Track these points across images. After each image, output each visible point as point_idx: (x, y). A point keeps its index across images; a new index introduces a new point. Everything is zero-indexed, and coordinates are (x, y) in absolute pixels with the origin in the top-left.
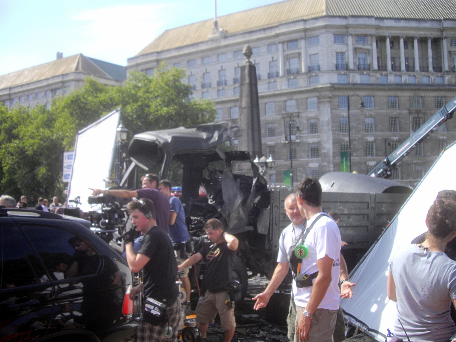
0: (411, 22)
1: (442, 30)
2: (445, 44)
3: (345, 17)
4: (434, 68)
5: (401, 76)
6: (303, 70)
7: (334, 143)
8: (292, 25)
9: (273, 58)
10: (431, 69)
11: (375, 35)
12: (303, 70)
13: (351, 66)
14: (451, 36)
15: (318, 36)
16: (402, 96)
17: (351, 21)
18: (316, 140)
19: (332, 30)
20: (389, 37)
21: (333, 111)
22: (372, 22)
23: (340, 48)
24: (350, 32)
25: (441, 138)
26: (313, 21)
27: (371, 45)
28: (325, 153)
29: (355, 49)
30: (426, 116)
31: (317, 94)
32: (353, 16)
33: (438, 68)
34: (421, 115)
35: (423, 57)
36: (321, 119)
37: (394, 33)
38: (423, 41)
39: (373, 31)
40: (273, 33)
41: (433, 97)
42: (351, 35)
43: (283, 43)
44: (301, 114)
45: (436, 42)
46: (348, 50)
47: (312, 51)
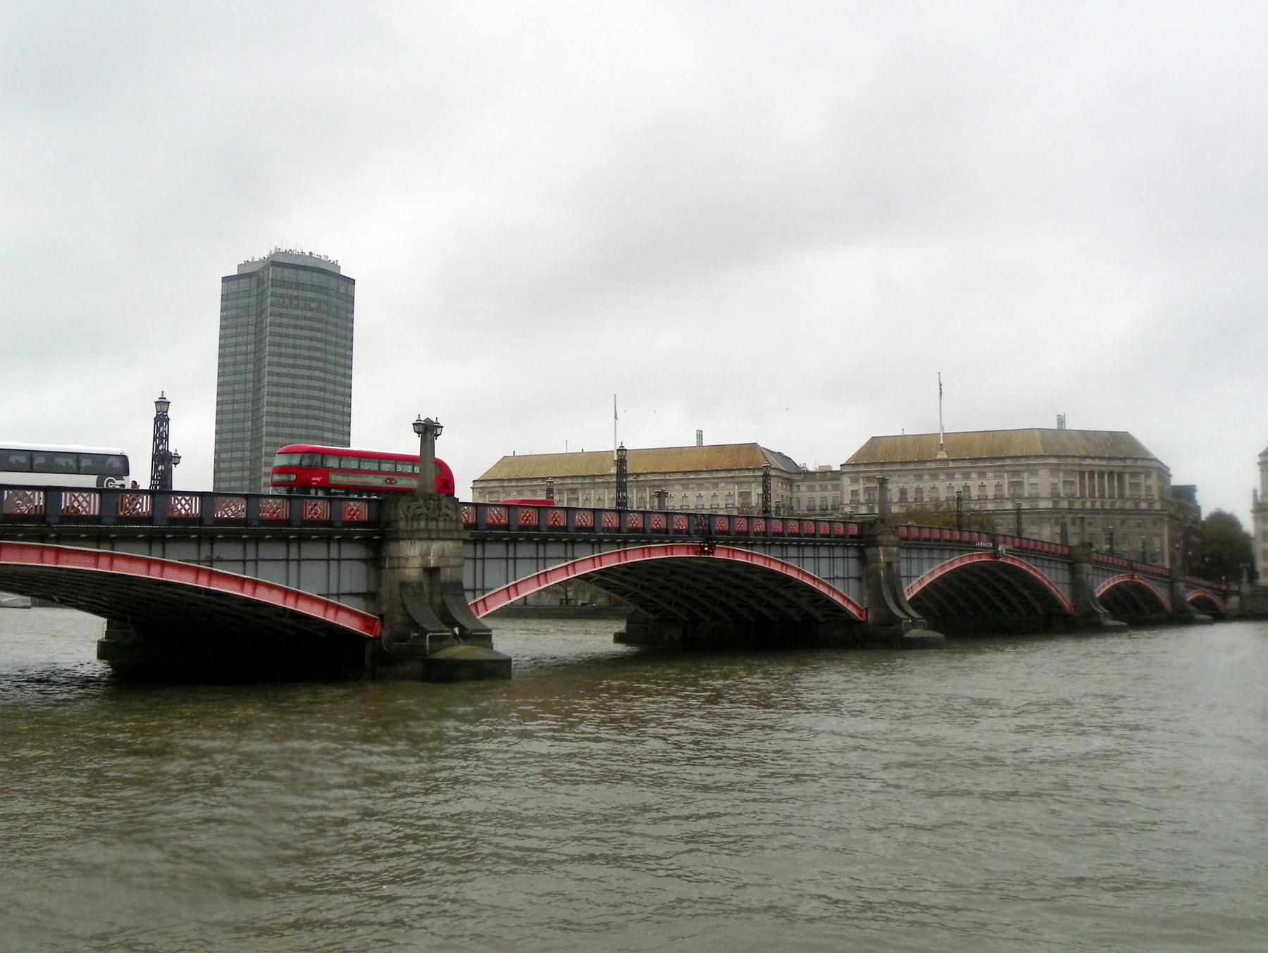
1: (1124, 467)
2: (1127, 478)
13: (1062, 494)
23: (1055, 480)
27: (1075, 478)
29: (1064, 481)
33: (1121, 496)
38: (1111, 474)
39: (1077, 468)
45: (1120, 475)
47: (1033, 480)
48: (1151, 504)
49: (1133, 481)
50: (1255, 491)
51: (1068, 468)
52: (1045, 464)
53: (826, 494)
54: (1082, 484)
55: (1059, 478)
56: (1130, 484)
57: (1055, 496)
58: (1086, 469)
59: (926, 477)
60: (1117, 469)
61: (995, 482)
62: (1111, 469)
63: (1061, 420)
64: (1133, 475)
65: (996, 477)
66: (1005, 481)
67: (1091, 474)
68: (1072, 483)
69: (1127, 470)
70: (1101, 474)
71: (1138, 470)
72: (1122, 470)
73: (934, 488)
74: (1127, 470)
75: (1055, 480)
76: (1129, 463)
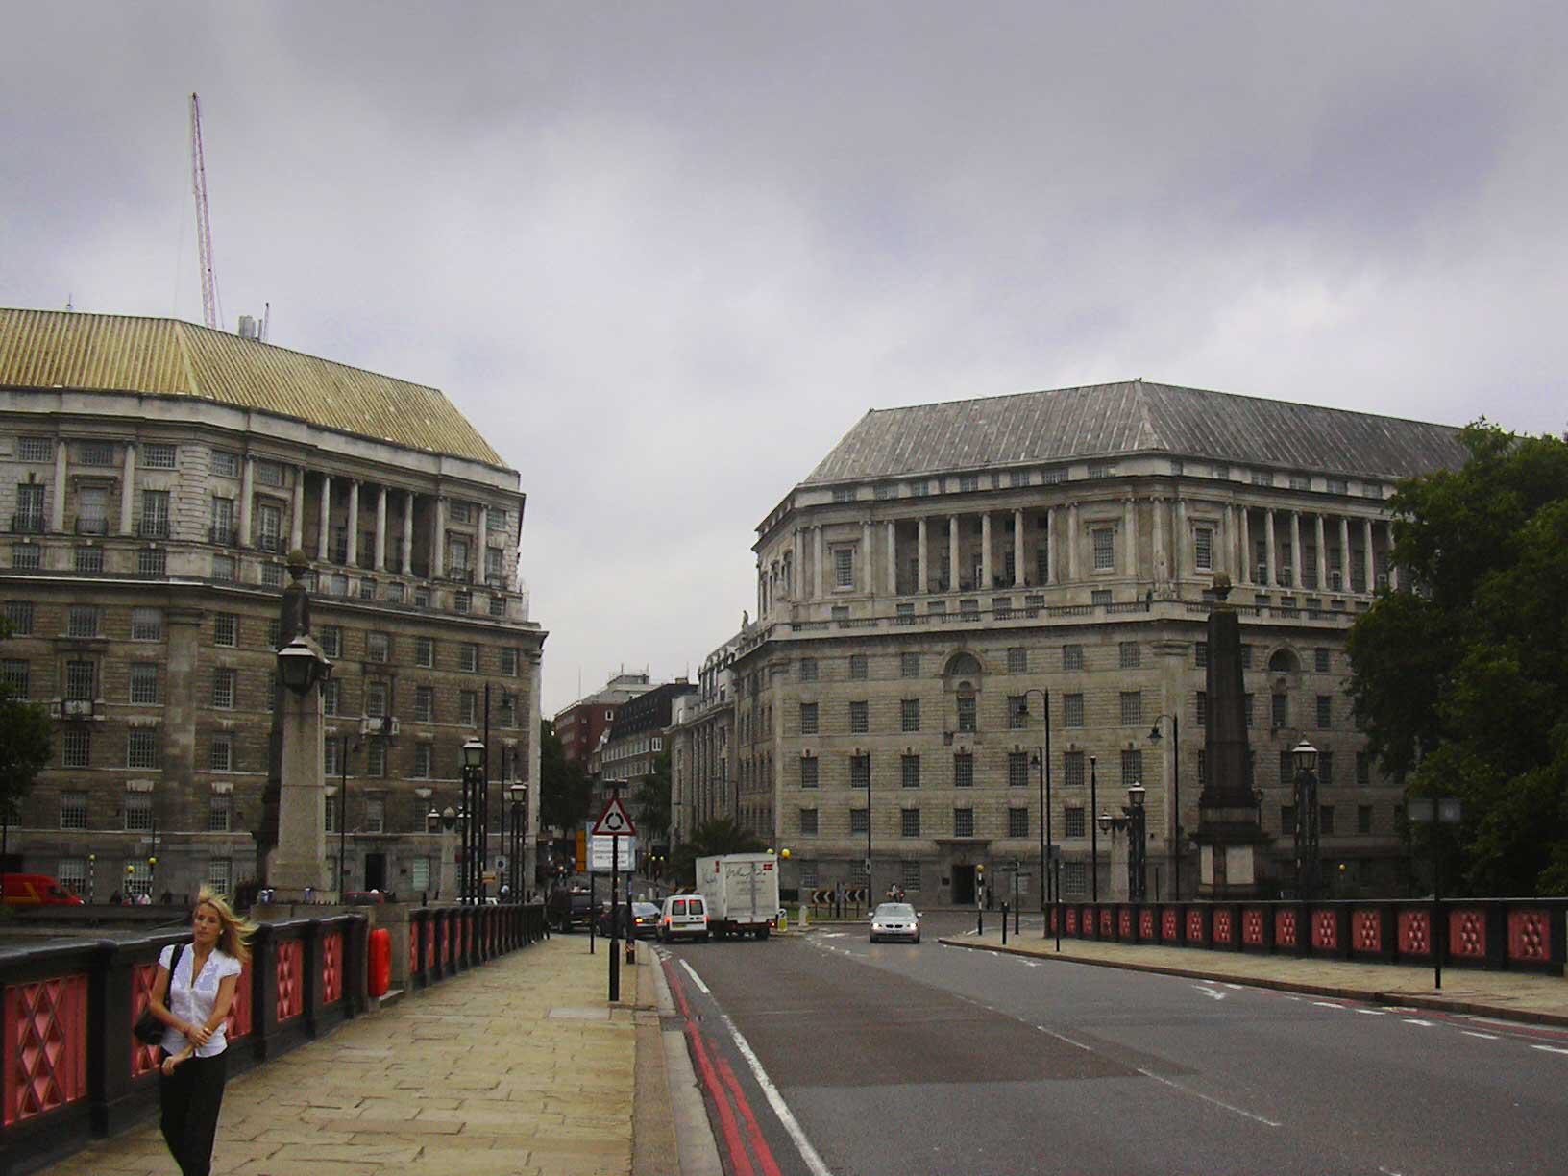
0: (378, 446)
1: (439, 479)
2: (442, 512)
3: (246, 411)
4: (413, 566)
5: (346, 577)
6: (127, 528)
7: (197, 732)
8: (103, 399)
9: (32, 476)
10: (407, 568)
11: (303, 468)
12: (127, 528)
13: (246, 540)
14: (454, 495)
15: (174, 446)
16: (349, 629)
17: (258, 426)
18: (151, 720)
19: (210, 438)
20: (329, 475)
21: (202, 650)
22: (301, 435)
23: (224, 487)
24: (252, 453)
25: (422, 735)
26: (164, 404)
28: (175, 757)
29: (257, 496)
30: (396, 680)
31: (163, 601)
32: (262, 413)
33: (422, 568)
34: (386, 679)
35: (396, 540)
36: (172, 667)
37: (341, 468)
38: (397, 497)
39: (300, 459)
40: (44, 406)
41: (413, 636)
42: (252, 457)
43: (69, 442)
44: (114, 648)
45: (425, 505)
46: (241, 495)
49: (455, 527)
51: (277, 453)
54: (312, 522)
55: (242, 482)
56: (447, 532)
57: (223, 541)
58: (326, 467)
61: (21, 474)
62: (401, 481)
64: (462, 508)
65: (24, 457)
66: (58, 471)
67: (341, 488)
68: (281, 507)
69: (444, 490)
74: (444, 490)
75: (224, 487)
76: (449, 468)
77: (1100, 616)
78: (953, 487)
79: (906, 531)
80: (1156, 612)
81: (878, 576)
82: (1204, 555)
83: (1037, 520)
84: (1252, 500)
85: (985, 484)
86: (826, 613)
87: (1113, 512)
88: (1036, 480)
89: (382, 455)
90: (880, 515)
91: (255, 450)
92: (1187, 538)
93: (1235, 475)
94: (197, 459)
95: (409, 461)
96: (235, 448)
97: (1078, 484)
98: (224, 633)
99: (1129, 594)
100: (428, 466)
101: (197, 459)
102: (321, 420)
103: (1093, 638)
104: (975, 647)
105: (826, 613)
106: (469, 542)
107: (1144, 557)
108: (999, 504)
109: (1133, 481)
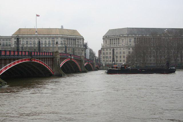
1: (76, 38)
2: (76, 40)
17: (63, 36)
22: (66, 36)
23: (61, 40)
33: (75, 44)
35: (73, 42)
37: (69, 38)
38: (73, 39)
39: (66, 38)
45: (75, 39)
48: (81, 46)
50: (102, 44)
52: (59, 37)
53: (4, 42)
54: (67, 41)
57: (62, 44)
58: (68, 38)
59: (33, 38)
60: (74, 38)
61: (48, 40)
63: (62, 27)
64: (78, 39)
66: (51, 40)
67: (69, 39)
70: (71, 39)
71: (79, 39)
72: (75, 38)
73: (34, 41)
74: (77, 38)
75: (61, 40)
76: (77, 37)
77: (122, 46)
78: (113, 36)
79: (110, 39)
80: (126, 46)
81: (108, 43)
82: (130, 41)
83: (118, 39)
84: (135, 37)
85: (115, 36)
86: (105, 46)
87: (123, 39)
88: (119, 36)
89: (72, 37)
90: (109, 38)
91: (63, 38)
92: (129, 40)
93: (133, 35)
94: (59, 39)
95: (74, 37)
96: (62, 38)
97: (121, 36)
98: (62, 50)
99: (124, 45)
100: (75, 37)
101: (59, 39)
102: (68, 35)
103: (122, 48)
104: (114, 48)
105: (105, 46)
106: (79, 42)
107: (125, 42)
108: (116, 38)
109: (125, 36)
